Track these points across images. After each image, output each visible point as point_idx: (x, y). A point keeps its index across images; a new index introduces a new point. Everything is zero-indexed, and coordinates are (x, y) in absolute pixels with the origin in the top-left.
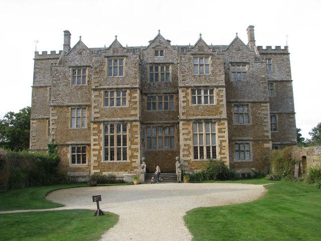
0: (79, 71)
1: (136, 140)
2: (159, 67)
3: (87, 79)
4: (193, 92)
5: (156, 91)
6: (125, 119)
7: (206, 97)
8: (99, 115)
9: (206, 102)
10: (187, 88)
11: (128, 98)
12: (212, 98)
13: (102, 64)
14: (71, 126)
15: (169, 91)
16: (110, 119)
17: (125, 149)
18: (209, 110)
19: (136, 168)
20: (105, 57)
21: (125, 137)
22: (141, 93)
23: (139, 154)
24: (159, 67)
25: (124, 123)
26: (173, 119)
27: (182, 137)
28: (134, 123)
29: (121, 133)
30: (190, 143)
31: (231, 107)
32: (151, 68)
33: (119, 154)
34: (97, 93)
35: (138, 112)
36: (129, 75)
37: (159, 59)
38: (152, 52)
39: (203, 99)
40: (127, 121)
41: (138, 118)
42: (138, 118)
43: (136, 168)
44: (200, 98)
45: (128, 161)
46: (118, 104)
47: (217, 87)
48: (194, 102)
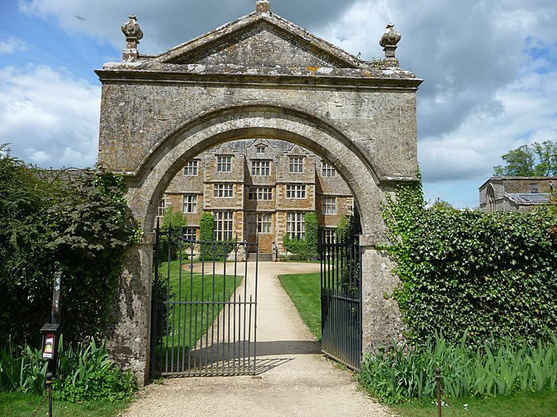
1: (240, 226)
2: (261, 163)
3: (198, 171)
4: (288, 188)
7: (299, 192)
8: (210, 204)
10: (284, 184)
12: (303, 193)
15: (269, 184)
16: (218, 208)
18: (302, 204)
20: (216, 155)
24: (261, 163)
25: (231, 212)
26: (270, 208)
27: (277, 224)
29: (228, 220)
30: (284, 229)
32: (254, 163)
34: (208, 186)
35: (242, 202)
37: (261, 156)
39: (296, 193)
40: (234, 210)
41: (242, 208)
42: (242, 208)
44: (294, 192)
46: (226, 195)
47: (309, 184)
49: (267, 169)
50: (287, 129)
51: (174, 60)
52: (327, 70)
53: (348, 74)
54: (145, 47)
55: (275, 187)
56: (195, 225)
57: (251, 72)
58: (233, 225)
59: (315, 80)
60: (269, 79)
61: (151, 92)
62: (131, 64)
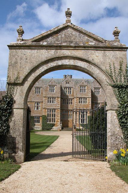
0: (38, 88)
3: (41, 92)
5: (66, 97)
6: (55, 108)
7: (84, 101)
8: (46, 106)
9: (84, 103)
10: (78, 97)
11: (56, 100)
13: (47, 87)
14: (35, 109)
17: (55, 119)
19: (58, 125)
21: (55, 114)
22: (61, 98)
23: (59, 121)
25: (55, 109)
28: (58, 110)
29: (53, 113)
31: (94, 104)
33: (52, 120)
35: (60, 105)
36: (57, 92)
37: (68, 85)
38: (65, 83)
40: (56, 109)
43: (58, 125)
44: (82, 101)
45: (56, 123)
48: (80, 103)
49: (71, 91)
50: (78, 65)
51: (35, 41)
52: (93, 43)
53: (101, 45)
54: (25, 37)
55: (74, 99)
56: (39, 115)
57: (64, 44)
58: (56, 115)
59: (88, 47)
60: (71, 47)
61: (28, 52)
62: (20, 42)
